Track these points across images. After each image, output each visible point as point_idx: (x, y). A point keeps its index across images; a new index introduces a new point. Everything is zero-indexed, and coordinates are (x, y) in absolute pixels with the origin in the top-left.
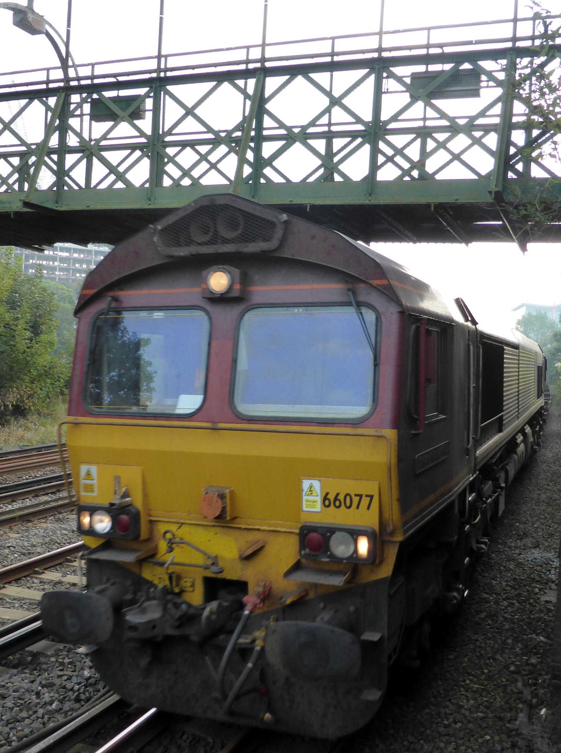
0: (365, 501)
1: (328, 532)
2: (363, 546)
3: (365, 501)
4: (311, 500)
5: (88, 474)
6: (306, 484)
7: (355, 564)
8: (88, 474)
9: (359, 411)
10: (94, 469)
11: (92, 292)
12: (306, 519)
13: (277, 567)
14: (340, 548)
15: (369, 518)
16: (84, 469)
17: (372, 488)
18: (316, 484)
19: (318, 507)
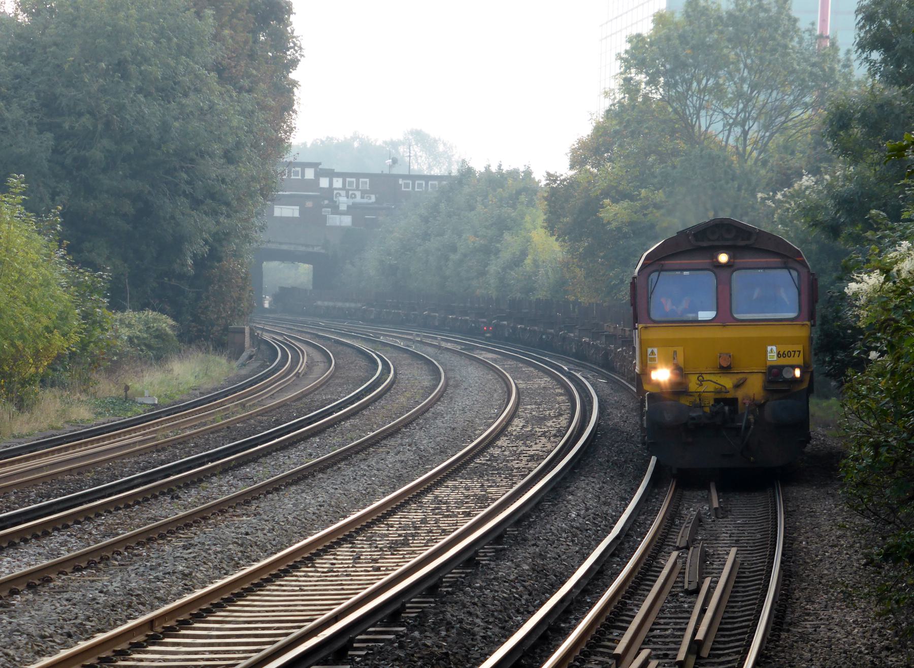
0: (797, 353)
1: (781, 368)
2: (798, 373)
3: (797, 353)
4: (772, 354)
5: (652, 352)
6: (769, 348)
7: (795, 380)
8: (652, 352)
9: (792, 315)
10: (655, 350)
11: (649, 262)
12: (769, 364)
13: (755, 387)
14: (786, 375)
15: (799, 360)
16: (650, 350)
17: (800, 348)
18: (774, 348)
19: (775, 358)
